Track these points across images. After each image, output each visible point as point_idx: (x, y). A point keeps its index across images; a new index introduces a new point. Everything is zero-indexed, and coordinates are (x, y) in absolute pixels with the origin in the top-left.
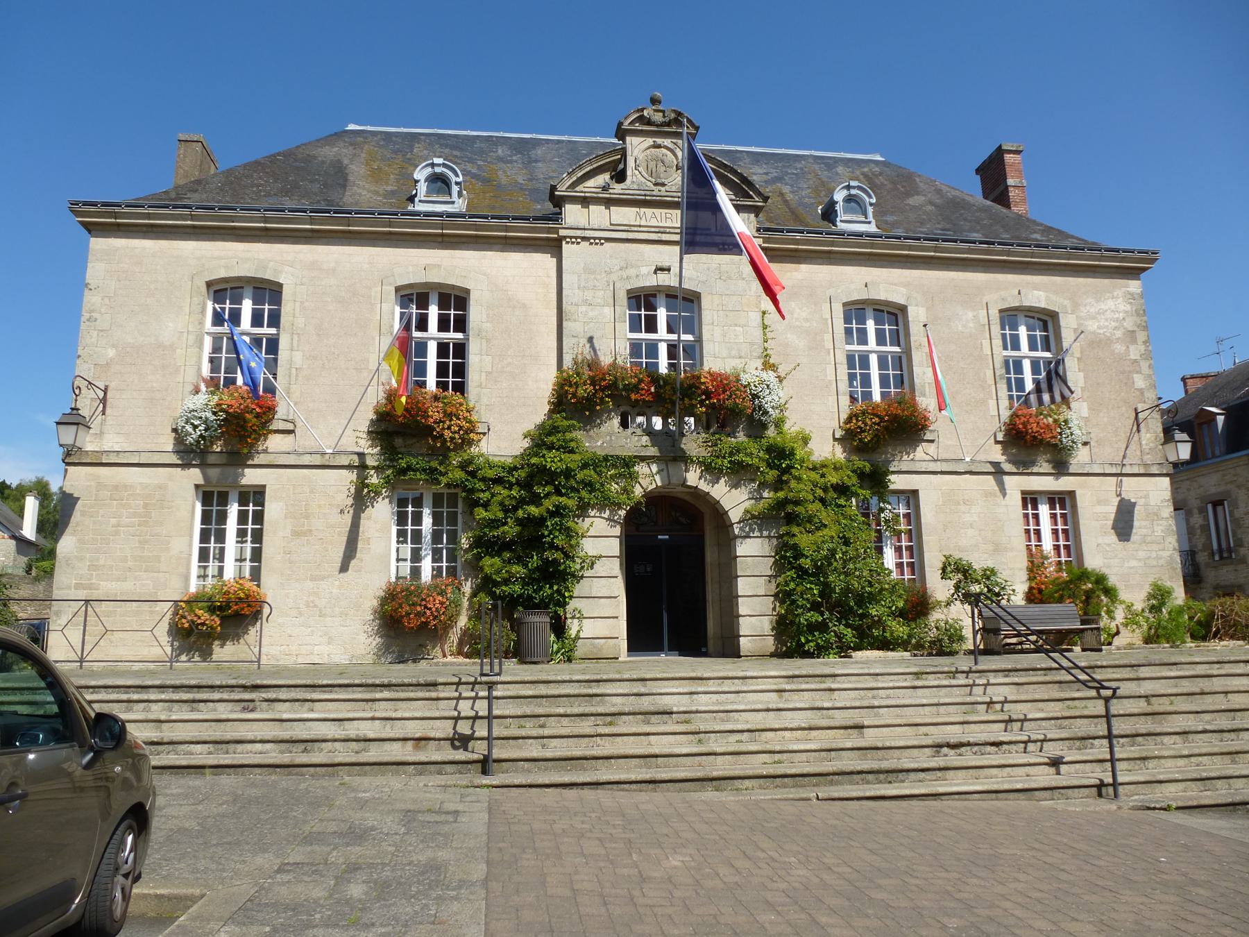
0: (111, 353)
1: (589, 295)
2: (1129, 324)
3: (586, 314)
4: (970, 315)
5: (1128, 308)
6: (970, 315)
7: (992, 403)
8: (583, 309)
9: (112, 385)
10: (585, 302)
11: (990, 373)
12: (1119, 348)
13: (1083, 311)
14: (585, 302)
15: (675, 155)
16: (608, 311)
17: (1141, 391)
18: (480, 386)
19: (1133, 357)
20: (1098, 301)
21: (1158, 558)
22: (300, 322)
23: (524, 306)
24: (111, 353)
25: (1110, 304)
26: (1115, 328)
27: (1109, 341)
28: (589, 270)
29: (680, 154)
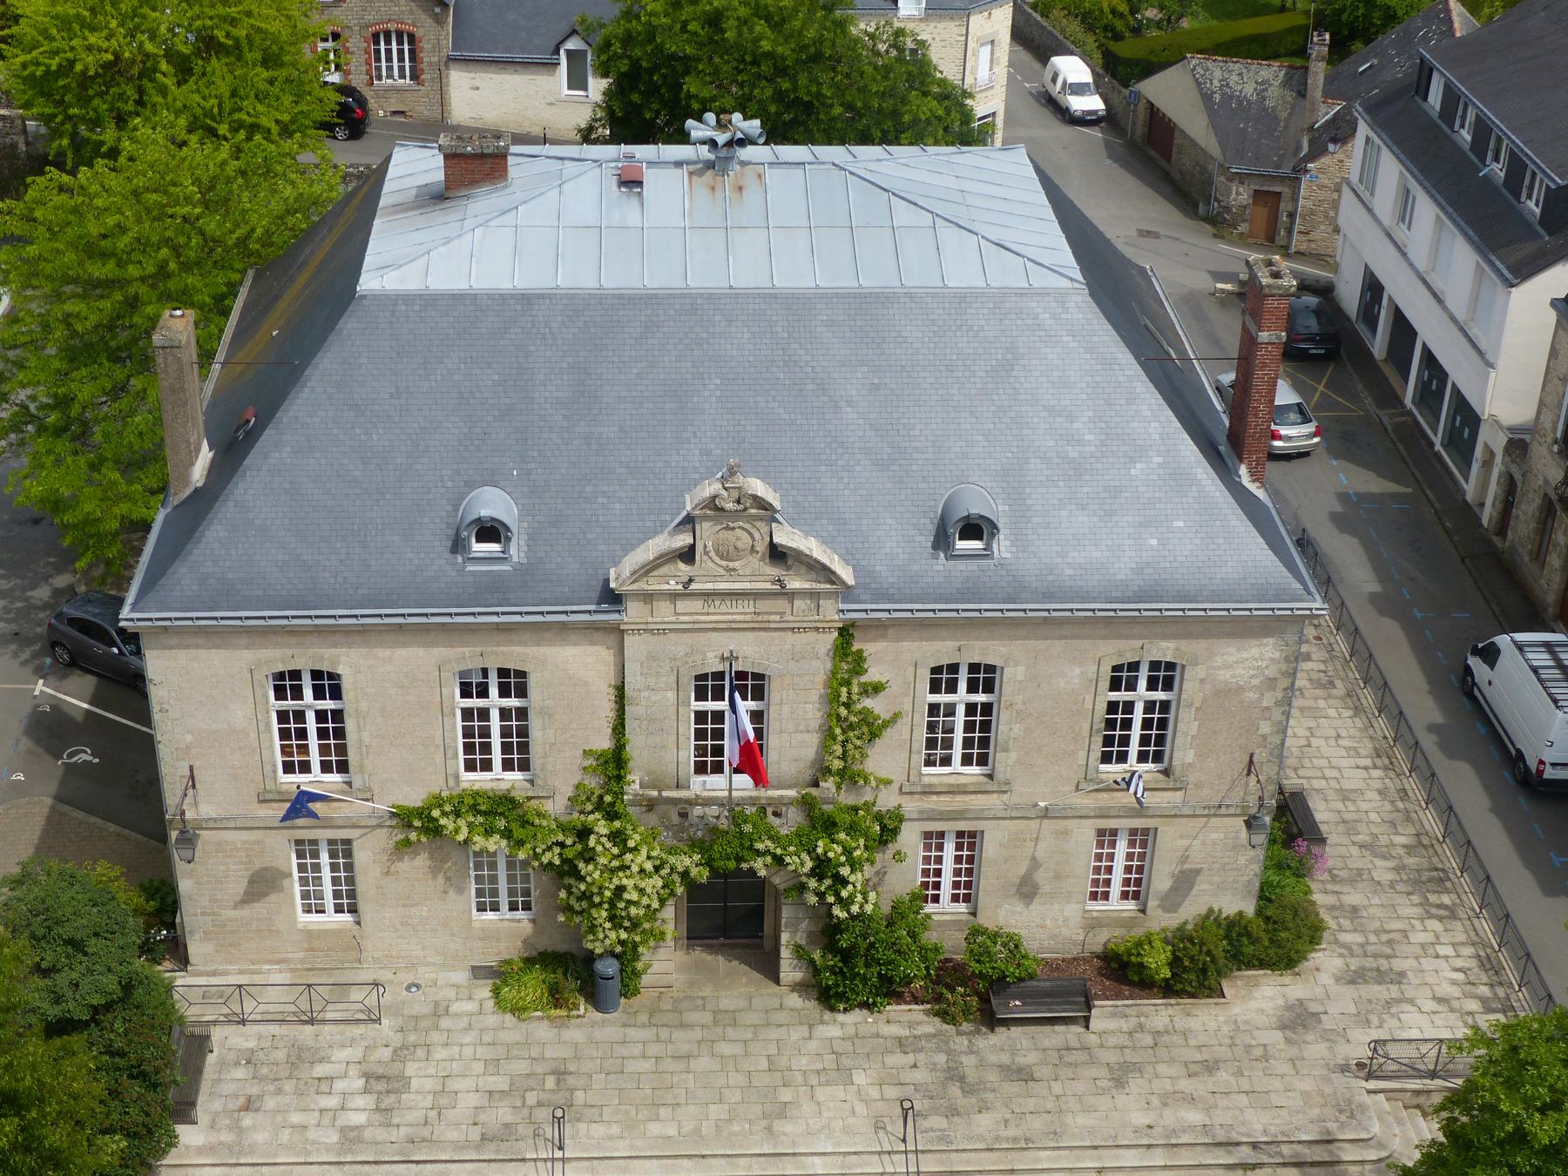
0: (189, 738)
1: (652, 682)
2: (1272, 672)
3: (648, 698)
4: (1078, 671)
5: (1277, 655)
6: (1078, 671)
7: (1082, 754)
8: (646, 694)
9: (197, 764)
10: (648, 687)
11: (1086, 727)
12: (1251, 696)
13: (1219, 661)
14: (648, 687)
15: (751, 534)
16: (671, 695)
17: (1264, 737)
18: (545, 756)
19: (1265, 704)
20: (1239, 650)
21: (1235, 882)
22: (364, 706)
23: (586, 683)
24: (189, 738)
25: (1255, 652)
26: (1252, 677)
27: (1241, 689)
28: (652, 657)
29: (757, 535)
